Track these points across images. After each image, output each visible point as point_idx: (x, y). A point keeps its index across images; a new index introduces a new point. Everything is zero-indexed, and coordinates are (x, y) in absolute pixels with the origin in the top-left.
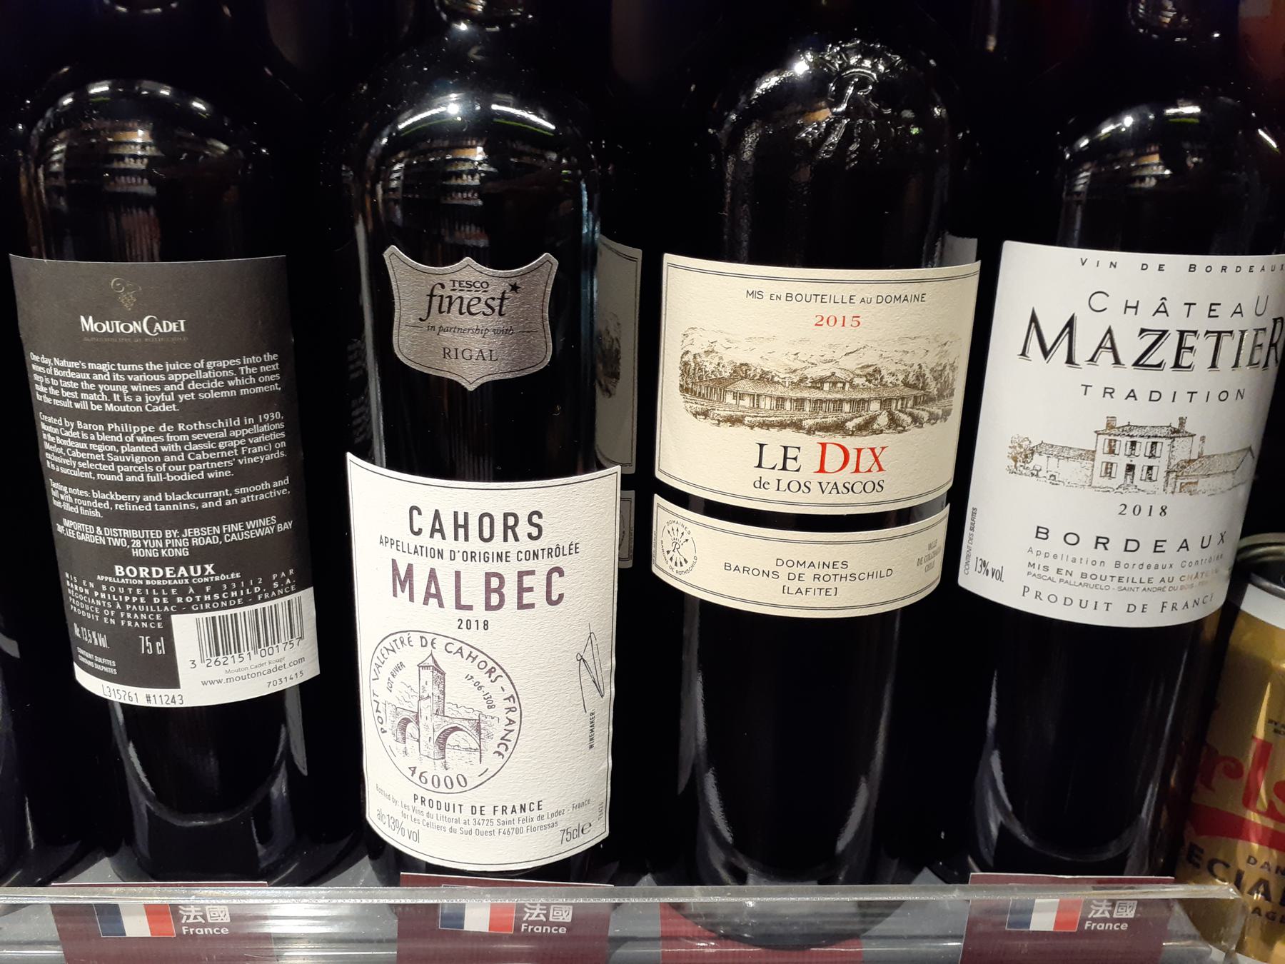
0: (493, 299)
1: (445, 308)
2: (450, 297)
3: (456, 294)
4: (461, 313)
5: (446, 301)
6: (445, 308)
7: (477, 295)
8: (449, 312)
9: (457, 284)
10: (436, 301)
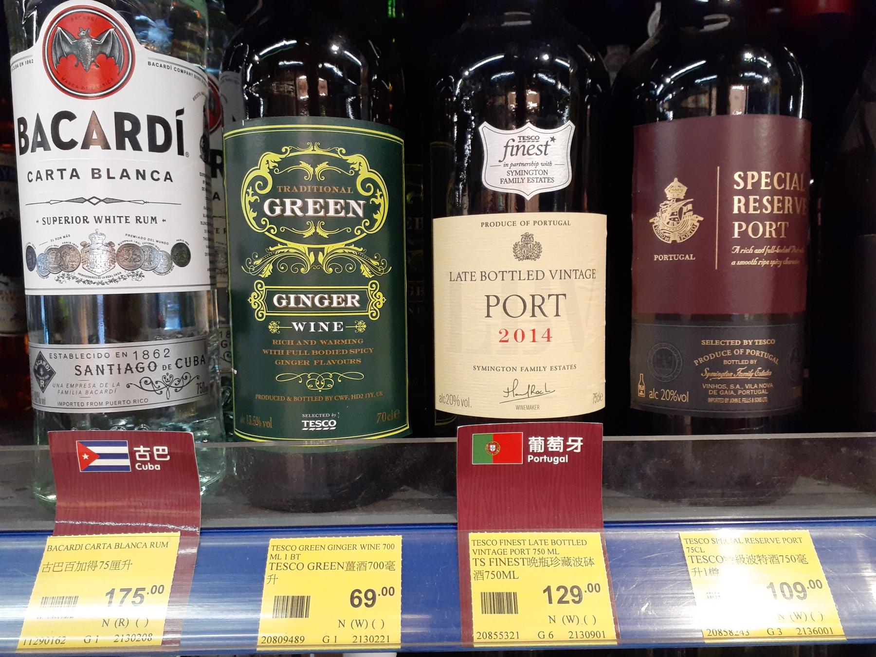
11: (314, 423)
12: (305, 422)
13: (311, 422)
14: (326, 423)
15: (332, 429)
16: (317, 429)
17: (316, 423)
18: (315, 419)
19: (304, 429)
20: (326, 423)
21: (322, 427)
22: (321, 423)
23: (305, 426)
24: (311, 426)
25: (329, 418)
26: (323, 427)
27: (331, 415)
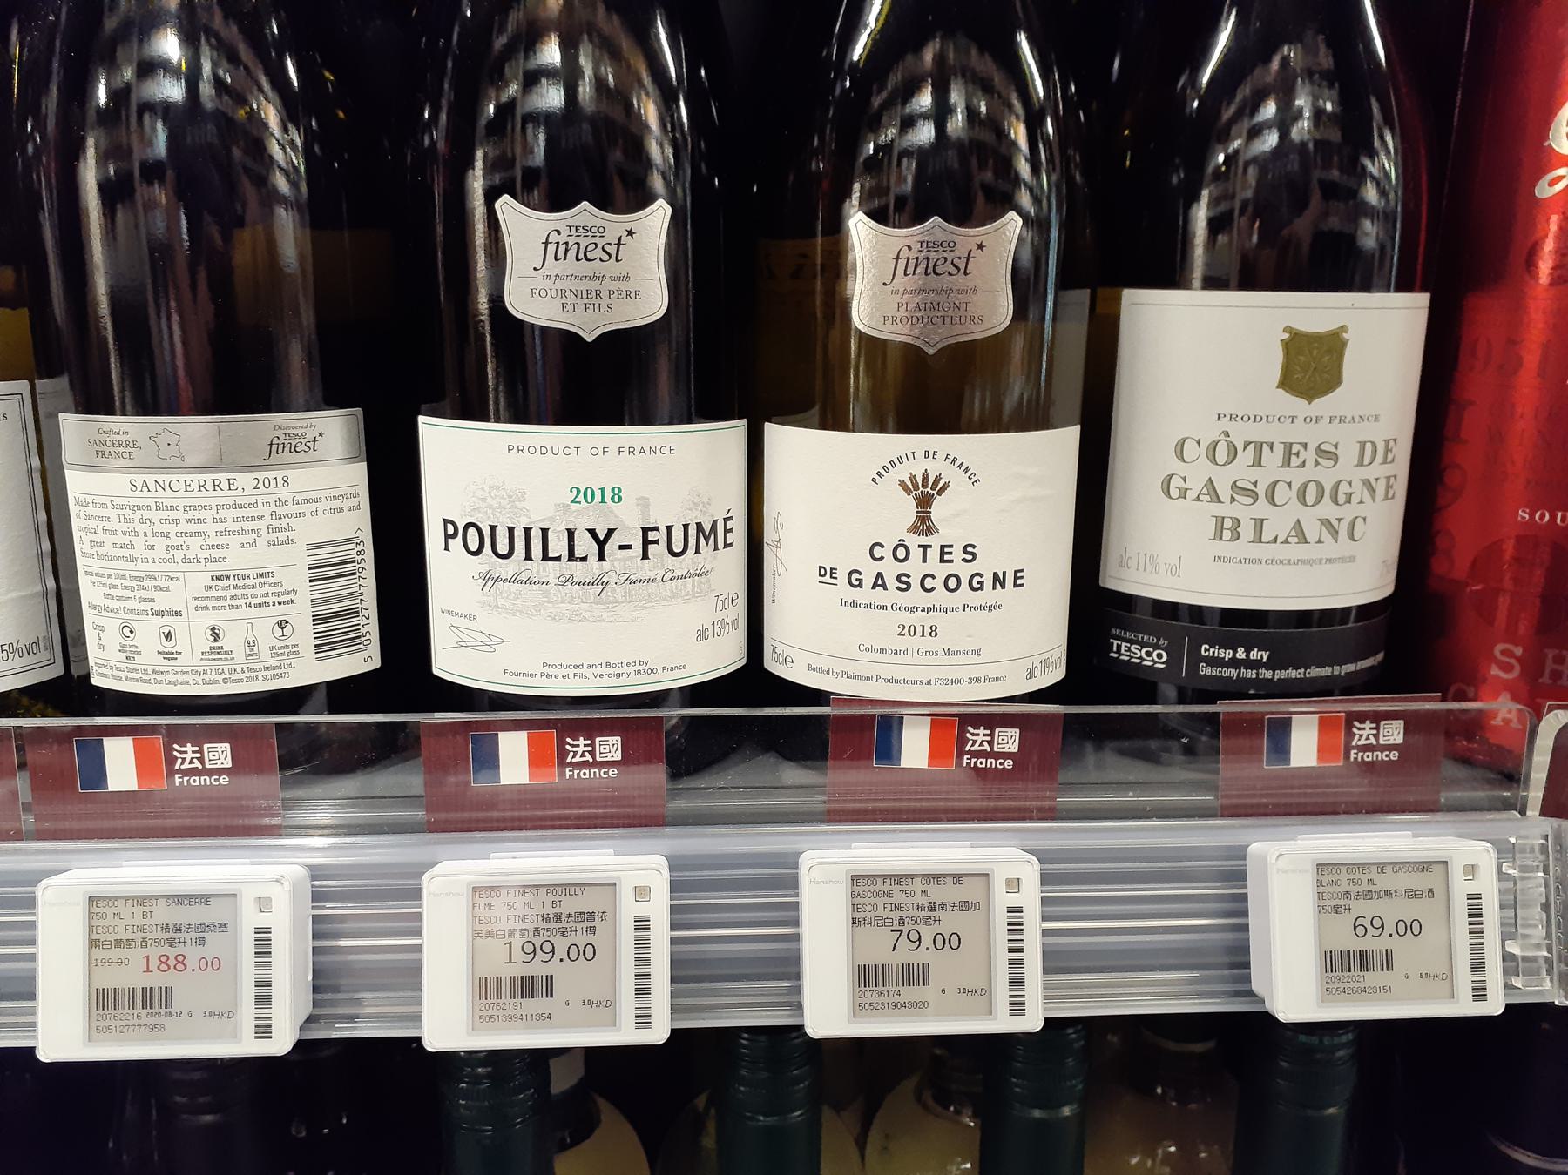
0: (610, 244)
1: (561, 254)
2: (567, 243)
3: (571, 241)
4: (577, 260)
5: (562, 249)
6: (561, 254)
7: (594, 240)
8: (565, 259)
9: (573, 229)
10: (551, 248)
11: (1129, 648)
12: (1115, 642)
13: (1124, 644)
14: (1148, 654)
15: (1157, 665)
16: (1133, 660)
17: (1132, 648)
18: (1131, 642)
19: (1112, 655)
20: (1148, 654)
21: (1141, 658)
22: (1140, 651)
23: (1115, 649)
24: (1123, 651)
25: (1156, 647)
26: (1143, 660)
27: (1159, 641)
